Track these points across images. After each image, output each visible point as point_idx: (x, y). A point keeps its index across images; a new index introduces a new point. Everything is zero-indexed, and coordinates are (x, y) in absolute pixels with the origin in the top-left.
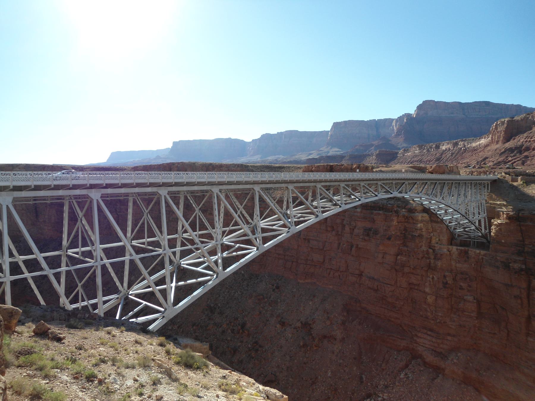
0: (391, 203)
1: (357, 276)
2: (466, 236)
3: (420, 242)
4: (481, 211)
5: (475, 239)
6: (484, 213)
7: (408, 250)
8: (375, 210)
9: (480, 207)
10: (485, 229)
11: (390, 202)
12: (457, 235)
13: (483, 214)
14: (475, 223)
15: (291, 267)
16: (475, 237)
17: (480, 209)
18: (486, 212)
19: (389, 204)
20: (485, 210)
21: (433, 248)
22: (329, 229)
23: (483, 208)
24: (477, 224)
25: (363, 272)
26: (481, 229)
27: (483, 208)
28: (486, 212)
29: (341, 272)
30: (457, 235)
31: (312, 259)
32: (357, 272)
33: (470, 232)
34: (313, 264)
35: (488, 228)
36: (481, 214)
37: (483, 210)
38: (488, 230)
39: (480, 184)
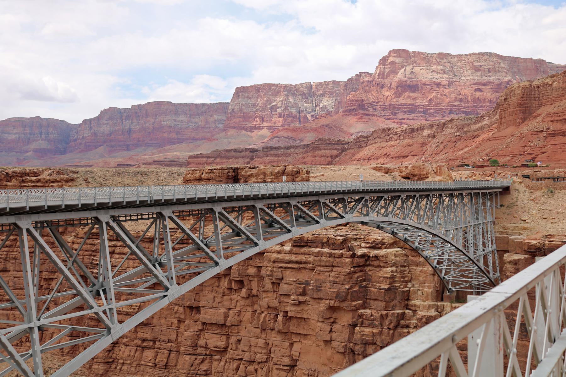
0: (342, 234)
1: (288, 368)
2: (466, 285)
3: (392, 300)
4: (486, 241)
5: (478, 289)
6: (492, 244)
7: (372, 316)
8: (316, 247)
9: (485, 234)
10: (495, 271)
11: (339, 232)
12: (450, 283)
13: (490, 246)
14: (478, 261)
15: (167, 363)
16: (478, 285)
17: (486, 238)
18: (494, 242)
19: (339, 236)
20: (494, 238)
21: (413, 309)
22: (234, 286)
23: (489, 236)
24: (481, 264)
25: (297, 360)
26: (488, 272)
27: (489, 236)
28: (494, 242)
29: (259, 363)
30: (450, 283)
31: (206, 345)
32: (287, 361)
33: (472, 278)
34: (208, 353)
35: (498, 268)
36: (487, 245)
37: (490, 239)
38: (498, 271)
39: (484, 194)
